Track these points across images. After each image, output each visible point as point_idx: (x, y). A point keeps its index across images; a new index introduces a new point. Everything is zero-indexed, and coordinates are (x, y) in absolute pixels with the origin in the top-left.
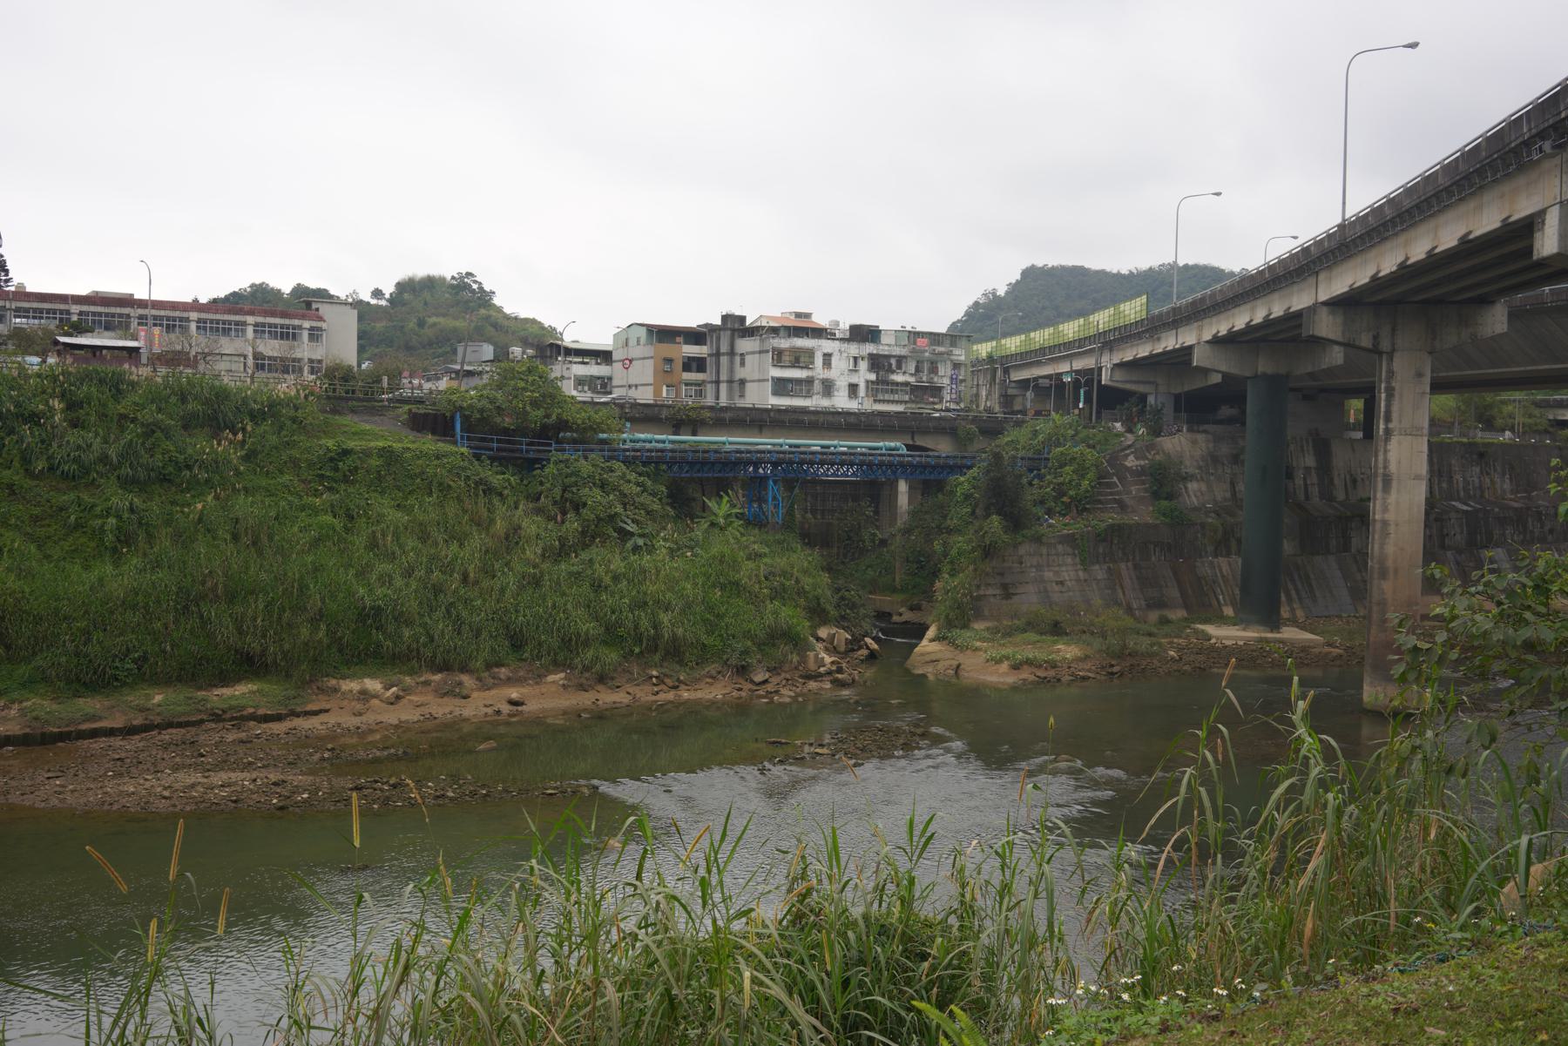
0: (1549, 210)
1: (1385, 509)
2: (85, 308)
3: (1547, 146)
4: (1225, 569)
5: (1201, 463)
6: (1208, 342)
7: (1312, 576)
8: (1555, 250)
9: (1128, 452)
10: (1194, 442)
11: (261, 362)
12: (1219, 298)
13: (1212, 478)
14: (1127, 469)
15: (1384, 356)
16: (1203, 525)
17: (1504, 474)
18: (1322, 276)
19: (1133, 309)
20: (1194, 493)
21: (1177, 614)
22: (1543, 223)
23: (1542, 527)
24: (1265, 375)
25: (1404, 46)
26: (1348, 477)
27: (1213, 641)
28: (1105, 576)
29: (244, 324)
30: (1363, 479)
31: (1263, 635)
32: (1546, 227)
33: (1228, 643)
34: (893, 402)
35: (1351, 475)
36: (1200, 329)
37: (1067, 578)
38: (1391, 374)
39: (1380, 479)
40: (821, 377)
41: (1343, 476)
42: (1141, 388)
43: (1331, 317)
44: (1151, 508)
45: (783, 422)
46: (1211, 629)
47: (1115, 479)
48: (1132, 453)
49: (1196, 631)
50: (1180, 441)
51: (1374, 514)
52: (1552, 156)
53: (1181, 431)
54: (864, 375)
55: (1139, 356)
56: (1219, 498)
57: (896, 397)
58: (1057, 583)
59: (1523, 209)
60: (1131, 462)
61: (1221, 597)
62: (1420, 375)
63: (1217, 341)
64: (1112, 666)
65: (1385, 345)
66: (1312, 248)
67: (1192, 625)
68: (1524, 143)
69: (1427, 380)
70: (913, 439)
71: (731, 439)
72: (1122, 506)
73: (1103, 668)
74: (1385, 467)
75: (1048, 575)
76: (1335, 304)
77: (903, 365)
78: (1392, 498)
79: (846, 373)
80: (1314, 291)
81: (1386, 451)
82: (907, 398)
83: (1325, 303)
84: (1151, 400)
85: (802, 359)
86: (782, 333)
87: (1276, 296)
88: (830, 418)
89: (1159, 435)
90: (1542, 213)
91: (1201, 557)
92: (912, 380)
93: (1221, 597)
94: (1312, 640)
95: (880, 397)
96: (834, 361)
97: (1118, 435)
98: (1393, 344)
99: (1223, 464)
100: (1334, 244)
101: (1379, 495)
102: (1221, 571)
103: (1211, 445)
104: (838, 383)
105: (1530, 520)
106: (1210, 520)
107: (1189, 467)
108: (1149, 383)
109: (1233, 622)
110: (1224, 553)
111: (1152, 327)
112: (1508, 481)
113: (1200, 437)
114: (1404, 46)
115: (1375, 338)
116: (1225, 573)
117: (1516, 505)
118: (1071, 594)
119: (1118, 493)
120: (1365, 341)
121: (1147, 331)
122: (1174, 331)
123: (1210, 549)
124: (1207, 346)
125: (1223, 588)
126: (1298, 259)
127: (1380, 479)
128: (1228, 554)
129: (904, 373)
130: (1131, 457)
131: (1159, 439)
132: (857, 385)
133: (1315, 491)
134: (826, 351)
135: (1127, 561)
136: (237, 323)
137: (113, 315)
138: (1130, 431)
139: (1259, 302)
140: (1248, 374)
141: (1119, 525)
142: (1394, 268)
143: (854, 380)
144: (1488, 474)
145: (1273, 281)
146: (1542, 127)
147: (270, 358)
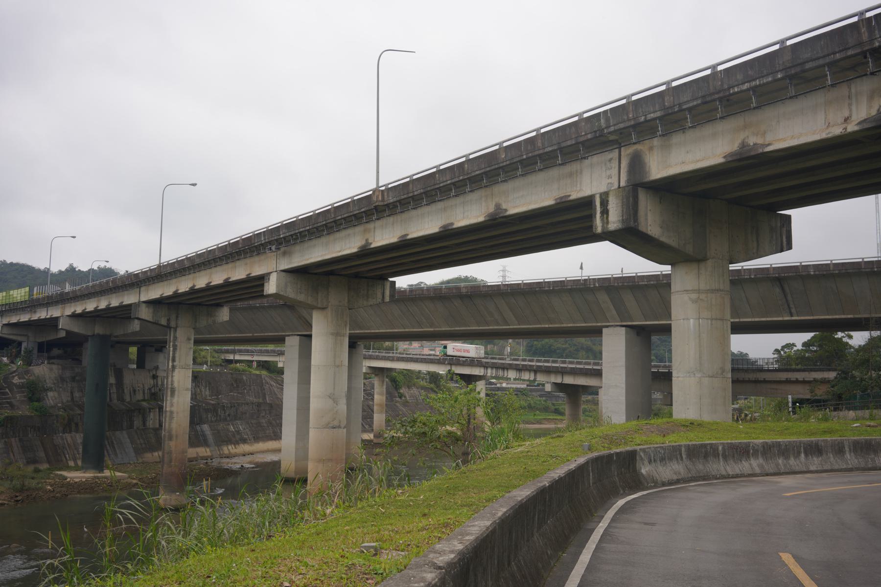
0: (271, 274)
1: (172, 405)
3: (273, 248)
4: (69, 439)
5: (55, 382)
6: (68, 316)
7: (115, 442)
8: (275, 292)
9: (14, 374)
10: (51, 370)
12: (78, 294)
13: (61, 389)
14: (15, 385)
15: (172, 330)
16: (57, 416)
17: (206, 387)
18: (142, 289)
19: (19, 294)
20: (51, 398)
21: (44, 466)
22: (269, 279)
23: (225, 413)
24: (99, 335)
25: (190, 185)
26: (131, 389)
27: (68, 480)
30: (139, 390)
31: (96, 475)
32: (270, 281)
33: (77, 480)
36: (64, 309)
38: (175, 338)
39: (169, 390)
41: (129, 388)
42: (19, 338)
43: (147, 309)
44: (28, 407)
46: (65, 473)
47: (7, 390)
48: (16, 375)
49: (57, 475)
50: (43, 368)
51: (166, 408)
52: (274, 252)
55: (21, 321)
56: (65, 401)
59: (257, 271)
60: (16, 380)
61: (67, 456)
62: (189, 339)
63: (74, 316)
64: (17, 496)
65: (173, 324)
66: (140, 275)
67: (54, 472)
68: (262, 244)
69: (192, 341)
72: (12, 406)
73: (12, 498)
74: (172, 385)
76: (149, 303)
78: (175, 400)
80: (138, 296)
81: (172, 376)
83: (144, 302)
84: (24, 345)
87: (114, 295)
89: (30, 365)
90: (269, 274)
91: (56, 434)
94: (121, 476)
97: (6, 365)
98: (177, 324)
99: (67, 382)
100: (153, 274)
101: (169, 398)
102: (67, 441)
103: (60, 371)
106: (61, 413)
107: (49, 384)
108: (24, 335)
109: (76, 468)
110: (68, 431)
111: (32, 305)
112: (208, 390)
113: (54, 367)
114: (190, 185)
115: (169, 320)
116: (69, 442)
117: (213, 402)
119: (9, 398)
120: (164, 322)
121: (28, 307)
122: (46, 309)
123: (61, 429)
124: (68, 318)
125: (69, 452)
126: (131, 279)
127: (169, 390)
128: (70, 432)
130: (16, 378)
131: (31, 368)
133: (115, 396)
135: (16, 437)
138: (12, 362)
139: (103, 298)
140: (89, 333)
141: (11, 417)
142: (187, 289)
144: (199, 387)
145: (114, 288)
146: (271, 239)
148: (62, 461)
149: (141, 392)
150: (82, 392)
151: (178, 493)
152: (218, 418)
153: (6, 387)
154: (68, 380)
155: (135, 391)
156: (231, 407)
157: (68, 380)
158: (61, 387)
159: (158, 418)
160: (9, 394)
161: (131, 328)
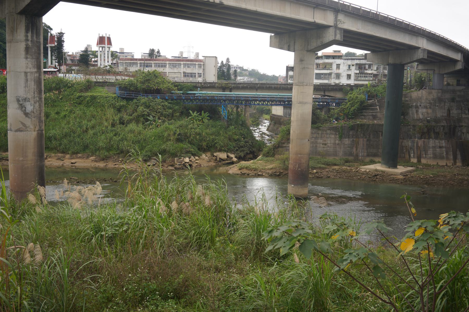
2: (141, 62)
5: (432, 101)
11: (185, 75)
13: (437, 107)
28: (350, 143)
29: (181, 64)
34: (364, 80)
37: (329, 143)
40: (336, 72)
45: (263, 87)
47: (378, 107)
50: (422, 93)
53: (426, 89)
54: (354, 71)
57: (367, 79)
58: (323, 144)
61: (412, 155)
70: (324, 93)
71: (280, 94)
75: (320, 141)
77: (371, 67)
79: (346, 71)
82: (371, 79)
85: (327, 66)
86: (323, 58)
88: (284, 86)
92: (375, 72)
93: (412, 155)
95: (359, 79)
96: (341, 67)
103: (440, 94)
104: (342, 74)
108: (432, 70)
116: (419, 145)
118: (328, 148)
129: (372, 70)
132: (350, 75)
134: (337, 63)
136: (179, 64)
137: (148, 63)
143: (349, 73)
147: (187, 73)
148: (404, 157)
150: (462, 110)
151: (293, 185)
153: (378, 105)
154: (447, 101)
157: (447, 101)
158: (437, 106)
160: (377, 110)
161: (416, 56)
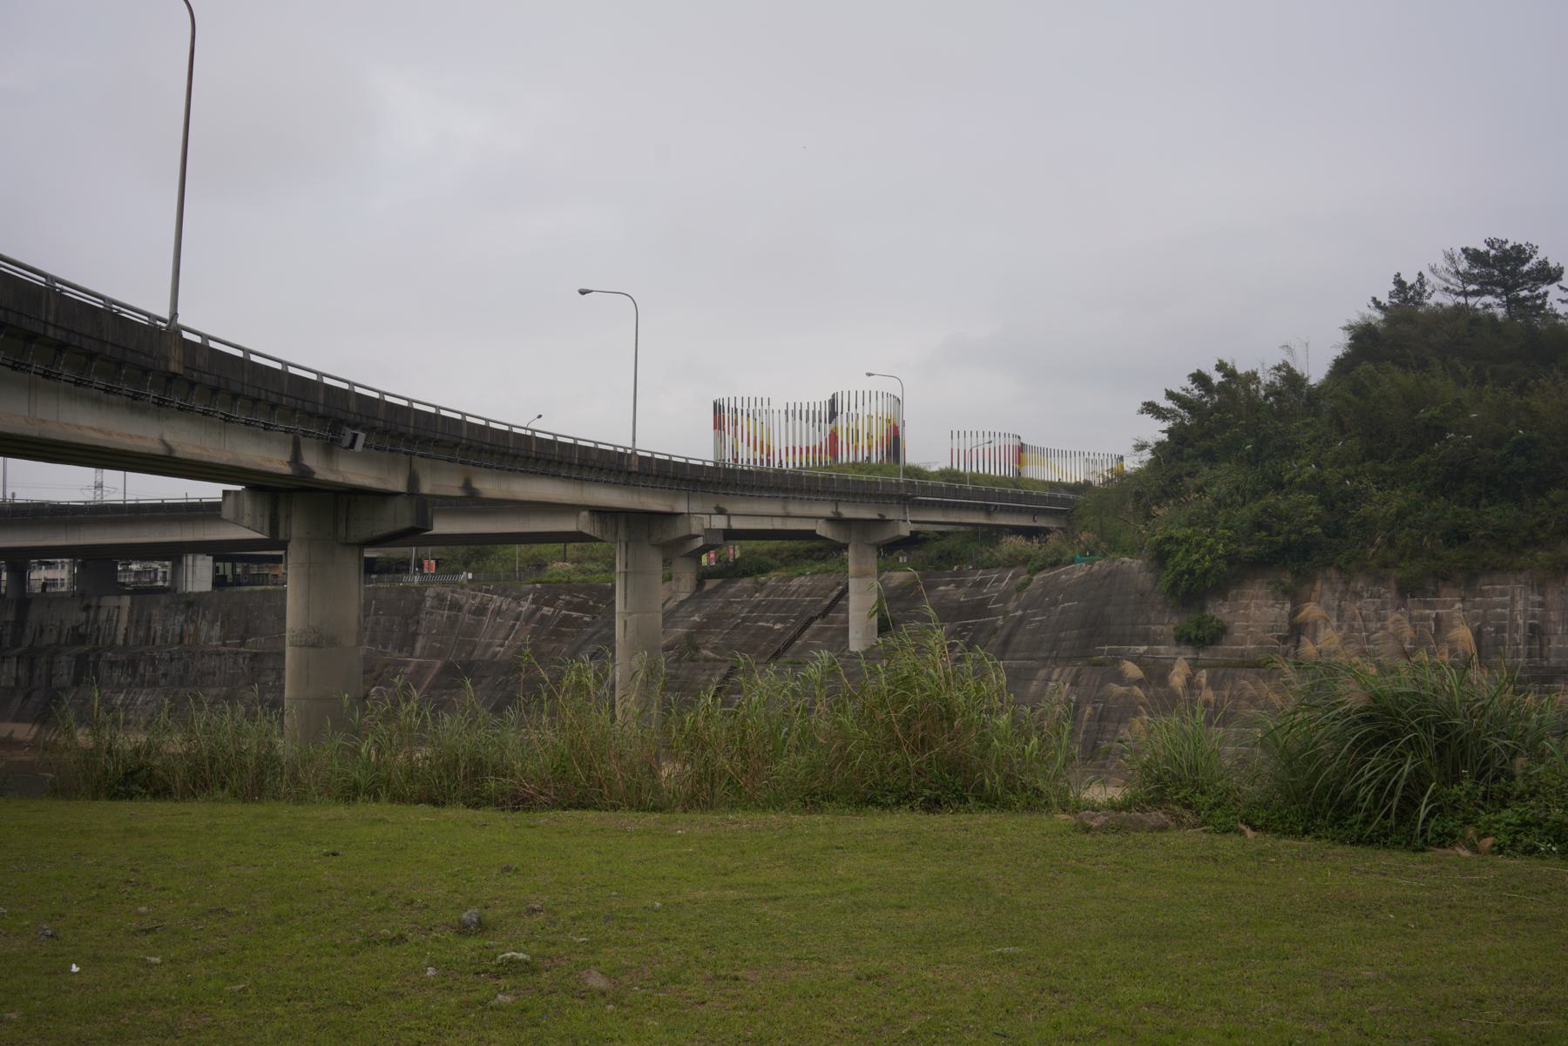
17: (214, 622)
23: (154, 671)
26: (38, 628)
30: (51, 630)
35: (41, 626)
41: (33, 628)
105: (142, 664)
144: (193, 621)
149: (55, 632)
152: (137, 680)
155: (42, 631)
156: (172, 660)
159: (14, 671)
